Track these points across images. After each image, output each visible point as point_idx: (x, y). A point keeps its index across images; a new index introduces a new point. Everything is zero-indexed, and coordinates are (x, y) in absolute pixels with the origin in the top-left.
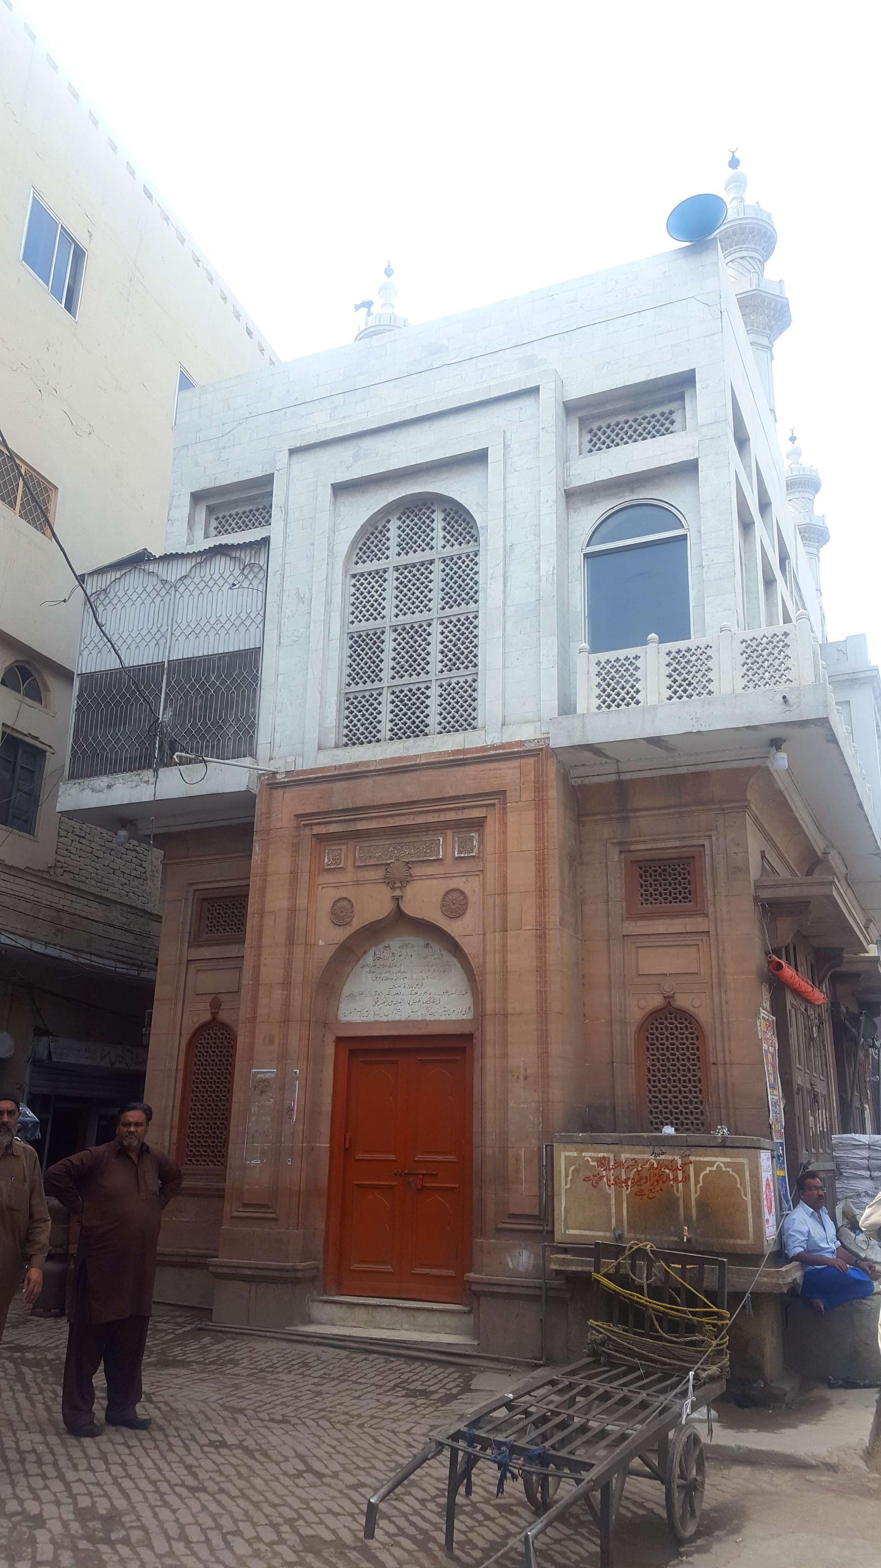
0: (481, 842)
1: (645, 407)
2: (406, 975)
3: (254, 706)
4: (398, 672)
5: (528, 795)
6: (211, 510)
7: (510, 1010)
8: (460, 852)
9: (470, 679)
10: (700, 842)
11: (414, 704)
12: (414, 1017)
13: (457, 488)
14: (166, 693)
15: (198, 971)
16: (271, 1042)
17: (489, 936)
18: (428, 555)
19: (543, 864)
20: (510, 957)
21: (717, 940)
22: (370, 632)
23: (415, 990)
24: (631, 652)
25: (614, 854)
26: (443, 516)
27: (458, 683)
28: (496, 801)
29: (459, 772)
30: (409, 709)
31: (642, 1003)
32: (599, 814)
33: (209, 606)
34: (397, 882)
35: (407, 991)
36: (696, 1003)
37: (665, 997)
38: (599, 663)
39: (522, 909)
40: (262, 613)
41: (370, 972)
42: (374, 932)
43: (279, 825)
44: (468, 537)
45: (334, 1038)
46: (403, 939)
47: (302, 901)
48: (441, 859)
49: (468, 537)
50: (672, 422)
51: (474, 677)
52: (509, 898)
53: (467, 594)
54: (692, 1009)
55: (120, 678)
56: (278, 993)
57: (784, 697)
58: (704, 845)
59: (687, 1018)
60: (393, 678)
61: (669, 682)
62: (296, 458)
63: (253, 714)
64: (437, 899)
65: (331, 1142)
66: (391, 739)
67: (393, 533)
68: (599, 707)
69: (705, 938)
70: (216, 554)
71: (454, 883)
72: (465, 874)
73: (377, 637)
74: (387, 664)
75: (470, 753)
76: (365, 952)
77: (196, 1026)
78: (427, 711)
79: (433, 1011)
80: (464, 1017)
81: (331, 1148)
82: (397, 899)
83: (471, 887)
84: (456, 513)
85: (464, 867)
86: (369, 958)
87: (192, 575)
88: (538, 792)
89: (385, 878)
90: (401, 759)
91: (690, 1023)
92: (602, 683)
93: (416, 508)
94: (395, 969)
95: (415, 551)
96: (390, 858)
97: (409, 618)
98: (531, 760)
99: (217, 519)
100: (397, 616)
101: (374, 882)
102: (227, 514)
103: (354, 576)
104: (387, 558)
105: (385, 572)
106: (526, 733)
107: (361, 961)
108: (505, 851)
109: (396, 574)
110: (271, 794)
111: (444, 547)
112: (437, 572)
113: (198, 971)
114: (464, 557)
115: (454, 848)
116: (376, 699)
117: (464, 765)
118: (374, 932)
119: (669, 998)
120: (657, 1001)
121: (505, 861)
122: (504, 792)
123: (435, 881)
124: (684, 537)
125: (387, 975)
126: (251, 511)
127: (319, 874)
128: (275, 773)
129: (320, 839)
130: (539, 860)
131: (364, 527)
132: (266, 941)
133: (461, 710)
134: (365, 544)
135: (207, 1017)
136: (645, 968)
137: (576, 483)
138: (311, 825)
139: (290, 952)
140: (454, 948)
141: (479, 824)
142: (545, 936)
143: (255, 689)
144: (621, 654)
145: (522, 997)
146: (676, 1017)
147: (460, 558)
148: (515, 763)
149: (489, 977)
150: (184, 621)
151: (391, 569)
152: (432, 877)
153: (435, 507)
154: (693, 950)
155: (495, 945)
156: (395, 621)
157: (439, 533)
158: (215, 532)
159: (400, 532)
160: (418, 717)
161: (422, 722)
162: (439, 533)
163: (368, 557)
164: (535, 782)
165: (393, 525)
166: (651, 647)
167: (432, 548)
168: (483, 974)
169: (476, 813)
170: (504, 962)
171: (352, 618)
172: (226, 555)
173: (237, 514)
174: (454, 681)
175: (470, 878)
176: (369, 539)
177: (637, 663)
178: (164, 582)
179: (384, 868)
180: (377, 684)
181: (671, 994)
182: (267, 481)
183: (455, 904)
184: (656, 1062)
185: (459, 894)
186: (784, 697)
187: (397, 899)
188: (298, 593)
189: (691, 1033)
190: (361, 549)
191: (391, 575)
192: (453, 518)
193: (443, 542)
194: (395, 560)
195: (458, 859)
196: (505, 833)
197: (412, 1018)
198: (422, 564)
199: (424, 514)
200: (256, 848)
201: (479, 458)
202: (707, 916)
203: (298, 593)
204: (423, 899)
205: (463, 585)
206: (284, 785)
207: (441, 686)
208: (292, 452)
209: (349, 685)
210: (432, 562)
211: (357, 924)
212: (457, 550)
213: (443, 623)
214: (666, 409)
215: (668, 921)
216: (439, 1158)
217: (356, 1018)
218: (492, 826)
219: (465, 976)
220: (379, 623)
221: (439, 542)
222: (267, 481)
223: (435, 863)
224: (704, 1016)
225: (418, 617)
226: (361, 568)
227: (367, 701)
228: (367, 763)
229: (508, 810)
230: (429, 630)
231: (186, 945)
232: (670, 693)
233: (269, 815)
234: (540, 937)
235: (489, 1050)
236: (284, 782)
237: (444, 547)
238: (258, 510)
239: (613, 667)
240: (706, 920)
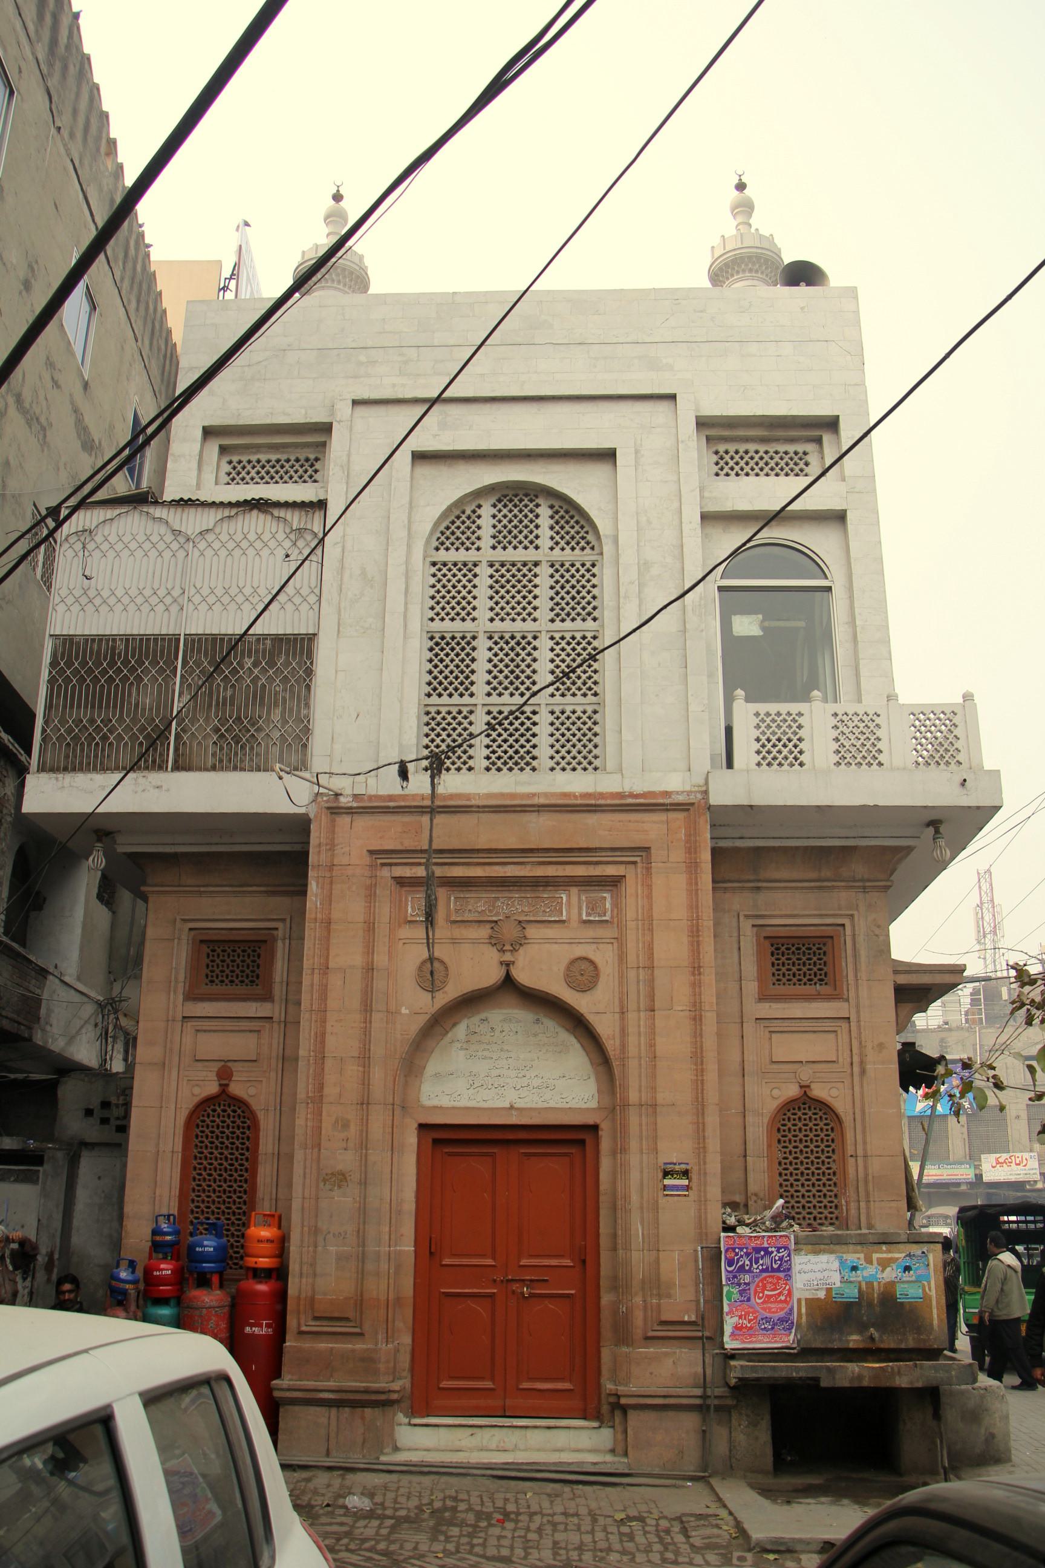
0: (616, 905)
1: (777, 440)
3: (307, 705)
4: (495, 689)
5: (678, 855)
6: (223, 450)
7: (660, 1101)
8: (588, 914)
9: (589, 709)
10: (840, 921)
11: (517, 730)
13: (579, 485)
14: (182, 676)
15: (198, 1031)
16: (346, 1125)
17: (631, 1016)
18: (531, 555)
19: (698, 936)
20: (660, 1041)
21: (859, 1027)
22: (456, 635)
23: (523, 1073)
24: (794, 708)
25: (747, 926)
26: (550, 512)
27: (574, 712)
28: (638, 859)
29: (591, 819)
30: (511, 735)
31: (776, 1092)
32: (730, 881)
33: (242, 573)
34: (506, 941)
35: (513, 1073)
36: (834, 1092)
37: (801, 1087)
38: (757, 714)
39: (675, 988)
40: (317, 591)
41: (462, 1049)
42: (472, 1001)
43: (345, 860)
44: (583, 543)
45: (416, 1125)
46: (505, 1011)
47: (381, 959)
48: (563, 922)
49: (583, 543)
50: (807, 464)
51: (596, 707)
52: (656, 972)
53: (584, 608)
54: (829, 1099)
55: (114, 648)
56: (353, 1070)
57: (965, 780)
58: (843, 925)
59: (824, 1108)
60: (489, 694)
61: (835, 746)
62: (361, 411)
63: (307, 716)
64: (560, 968)
65: (415, 1246)
66: (488, 769)
67: (486, 522)
68: (759, 764)
69: (845, 1025)
70: (251, 510)
71: (579, 951)
72: (596, 941)
73: (467, 642)
74: (481, 677)
75: (603, 798)
76: (455, 1025)
77: (196, 1100)
78: (534, 741)
81: (416, 1251)
82: (508, 965)
83: (605, 957)
84: (567, 512)
85: (590, 932)
86: (461, 1030)
87: (217, 530)
88: (690, 853)
89: (491, 937)
90: (512, 796)
91: (825, 1114)
92: (761, 737)
93: (513, 495)
95: (515, 548)
96: (497, 914)
97: (507, 626)
98: (681, 816)
99: (230, 462)
100: (492, 620)
101: (475, 942)
102: (245, 459)
103: (434, 564)
104: (478, 549)
105: (475, 565)
106: (675, 783)
107: (450, 1035)
108: (651, 918)
109: (491, 571)
110: (333, 821)
111: (552, 549)
112: (544, 579)
113: (198, 1031)
114: (578, 565)
115: (580, 908)
116: (465, 718)
117: (595, 811)
118: (472, 1001)
119: (805, 1087)
120: (792, 1091)
121: (651, 930)
122: (647, 849)
123: (556, 946)
124: (829, 589)
125: (486, 1053)
126: (278, 461)
127: (400, 926)
128: (337, 795)
129: (401, 882)
130: (692, 932)
131: (449, 509)
132: (332, 1003)
133: (580, 743)
134: (448, 528)
135: (213, 1088)
136: (780, 1055)
137: (712, 508)
138: (390, 865)
139: (367, 1022)
140: (577, 1023)
141: (614, 883)
142: (701, 1020)
143: (308, 687)
144: (784, 708)
145: (674, 1086)
146: (810, 1108)
147: (573, 565)
148: (662, 817)
149: (633, 1064)
150: (206, 586)
151: (484, 564)
152: (554, 941)
153: (539, 501)
154: (832, 1035)
155: (639, 1026)
156: (490, 627)
157: (545, 532)
158: (227, 479)
159: (494, 521)
160: (522, 746)
161: (528, 752)
162: (545, 532)
163: (453, 544)
164: (687, 842)
165: (487, 511)
166: (817, 705)
167: (537, 548)
168: (623, 1059)
169: (611, 871)
170: (652, 1045)
171: (431, 614)
172: (265, 512)
173: (259, 461)
174: (568, 709)
175: (601, 946)
176: (453, 523)
177: (801, 720)
178: (177, 533)
179: (488, 926)
180: (466, 699)
181: (807, 1083)
182: (326, 428)
183: (583, 974)
184: (787, 1155)
185: (588, 964)
186: (965, 780)
187: (508, 965)
188: (363, 573)
189: (826, 1125)
190: (443, 533)
191: (484, 571)
192: (562, 517)
193: (551, 543)
194: (487, 554)
195: (585, 922)
196: (650, 897)
198: (525, 564)
199: (526, 506)
200: (313, 887)
201: (608, 456)
202: (847, 1000)
203: (363, 573)
204: (542, 966)
205: (577, 594)
206: (350, 811)
207: (552, 713)
208: (355, 403)
209: (429, 695)
210: (536, 564)
211: (452, 992)
212: (568, 555)
213: (552, 638)
214: (800, 448)
215: (806, 1004)
216: (554, 1262)
217: (445, 1102)
218: (632, 886)
219: (586, 1059)
220: (468, 625)
221: (545, 542)
222: (326, 428)
223: (556, 925)
224: (841, 1106)
225: (519, 626)
226: (442, 556)
227: (454, 718)
228: (468, 797)
229: (653, 870)
230: (535, 643)
231: (181, 997)
232: (836, 758)
233: (332, 846)
234: (694, 1019)
235: (634, 1144)
236: (351, 808)
237: (552, 549)
238: (288, 461)
239: (773, 721)
240: (846, 1004)
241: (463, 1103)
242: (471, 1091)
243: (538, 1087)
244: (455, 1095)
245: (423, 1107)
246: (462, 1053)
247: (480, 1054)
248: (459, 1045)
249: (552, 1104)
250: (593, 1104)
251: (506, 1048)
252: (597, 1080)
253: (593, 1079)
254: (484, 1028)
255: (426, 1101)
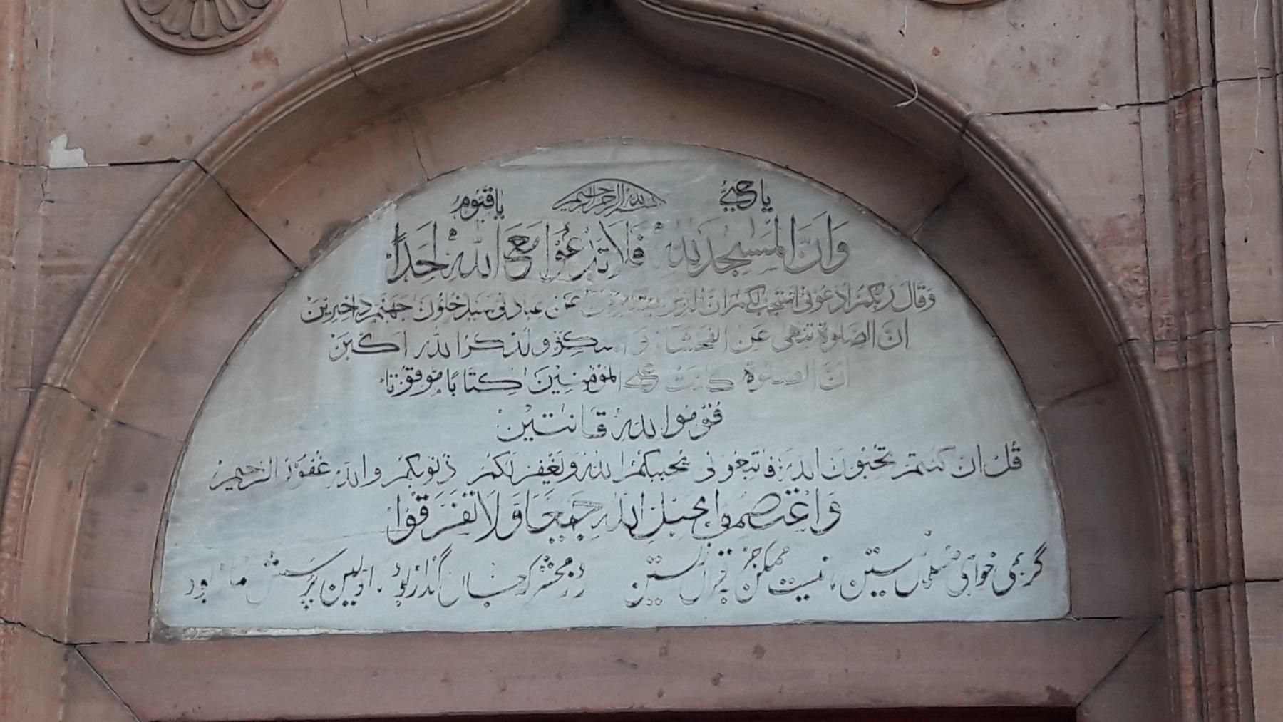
2: (605, 363)
12: (665, 608)
35: (619, 455)
41: (368, 346)
76: (334, 233)
79: (797, 567)
80: (992, 610)
94: (533, 331)
107: (309, 284)
125: (485, 362)
140: (948, 187)
197: (647, 617)
241: (375, 612)
242: (414, 550)
243: (748, 522)
244: (333, 574)
245: (166, 637)
246: (368, 365)
247: (456, 364)
248: (355, 331)
249: (824, 605)
250: (1044, 599)
251: (585, 330)
252: (1060, 474)
253: (1035, 469)
254: (479, 238)
255: (185, 610)
